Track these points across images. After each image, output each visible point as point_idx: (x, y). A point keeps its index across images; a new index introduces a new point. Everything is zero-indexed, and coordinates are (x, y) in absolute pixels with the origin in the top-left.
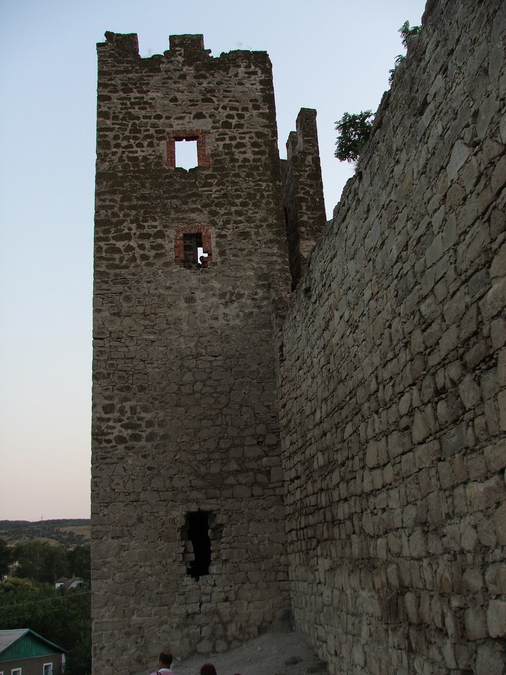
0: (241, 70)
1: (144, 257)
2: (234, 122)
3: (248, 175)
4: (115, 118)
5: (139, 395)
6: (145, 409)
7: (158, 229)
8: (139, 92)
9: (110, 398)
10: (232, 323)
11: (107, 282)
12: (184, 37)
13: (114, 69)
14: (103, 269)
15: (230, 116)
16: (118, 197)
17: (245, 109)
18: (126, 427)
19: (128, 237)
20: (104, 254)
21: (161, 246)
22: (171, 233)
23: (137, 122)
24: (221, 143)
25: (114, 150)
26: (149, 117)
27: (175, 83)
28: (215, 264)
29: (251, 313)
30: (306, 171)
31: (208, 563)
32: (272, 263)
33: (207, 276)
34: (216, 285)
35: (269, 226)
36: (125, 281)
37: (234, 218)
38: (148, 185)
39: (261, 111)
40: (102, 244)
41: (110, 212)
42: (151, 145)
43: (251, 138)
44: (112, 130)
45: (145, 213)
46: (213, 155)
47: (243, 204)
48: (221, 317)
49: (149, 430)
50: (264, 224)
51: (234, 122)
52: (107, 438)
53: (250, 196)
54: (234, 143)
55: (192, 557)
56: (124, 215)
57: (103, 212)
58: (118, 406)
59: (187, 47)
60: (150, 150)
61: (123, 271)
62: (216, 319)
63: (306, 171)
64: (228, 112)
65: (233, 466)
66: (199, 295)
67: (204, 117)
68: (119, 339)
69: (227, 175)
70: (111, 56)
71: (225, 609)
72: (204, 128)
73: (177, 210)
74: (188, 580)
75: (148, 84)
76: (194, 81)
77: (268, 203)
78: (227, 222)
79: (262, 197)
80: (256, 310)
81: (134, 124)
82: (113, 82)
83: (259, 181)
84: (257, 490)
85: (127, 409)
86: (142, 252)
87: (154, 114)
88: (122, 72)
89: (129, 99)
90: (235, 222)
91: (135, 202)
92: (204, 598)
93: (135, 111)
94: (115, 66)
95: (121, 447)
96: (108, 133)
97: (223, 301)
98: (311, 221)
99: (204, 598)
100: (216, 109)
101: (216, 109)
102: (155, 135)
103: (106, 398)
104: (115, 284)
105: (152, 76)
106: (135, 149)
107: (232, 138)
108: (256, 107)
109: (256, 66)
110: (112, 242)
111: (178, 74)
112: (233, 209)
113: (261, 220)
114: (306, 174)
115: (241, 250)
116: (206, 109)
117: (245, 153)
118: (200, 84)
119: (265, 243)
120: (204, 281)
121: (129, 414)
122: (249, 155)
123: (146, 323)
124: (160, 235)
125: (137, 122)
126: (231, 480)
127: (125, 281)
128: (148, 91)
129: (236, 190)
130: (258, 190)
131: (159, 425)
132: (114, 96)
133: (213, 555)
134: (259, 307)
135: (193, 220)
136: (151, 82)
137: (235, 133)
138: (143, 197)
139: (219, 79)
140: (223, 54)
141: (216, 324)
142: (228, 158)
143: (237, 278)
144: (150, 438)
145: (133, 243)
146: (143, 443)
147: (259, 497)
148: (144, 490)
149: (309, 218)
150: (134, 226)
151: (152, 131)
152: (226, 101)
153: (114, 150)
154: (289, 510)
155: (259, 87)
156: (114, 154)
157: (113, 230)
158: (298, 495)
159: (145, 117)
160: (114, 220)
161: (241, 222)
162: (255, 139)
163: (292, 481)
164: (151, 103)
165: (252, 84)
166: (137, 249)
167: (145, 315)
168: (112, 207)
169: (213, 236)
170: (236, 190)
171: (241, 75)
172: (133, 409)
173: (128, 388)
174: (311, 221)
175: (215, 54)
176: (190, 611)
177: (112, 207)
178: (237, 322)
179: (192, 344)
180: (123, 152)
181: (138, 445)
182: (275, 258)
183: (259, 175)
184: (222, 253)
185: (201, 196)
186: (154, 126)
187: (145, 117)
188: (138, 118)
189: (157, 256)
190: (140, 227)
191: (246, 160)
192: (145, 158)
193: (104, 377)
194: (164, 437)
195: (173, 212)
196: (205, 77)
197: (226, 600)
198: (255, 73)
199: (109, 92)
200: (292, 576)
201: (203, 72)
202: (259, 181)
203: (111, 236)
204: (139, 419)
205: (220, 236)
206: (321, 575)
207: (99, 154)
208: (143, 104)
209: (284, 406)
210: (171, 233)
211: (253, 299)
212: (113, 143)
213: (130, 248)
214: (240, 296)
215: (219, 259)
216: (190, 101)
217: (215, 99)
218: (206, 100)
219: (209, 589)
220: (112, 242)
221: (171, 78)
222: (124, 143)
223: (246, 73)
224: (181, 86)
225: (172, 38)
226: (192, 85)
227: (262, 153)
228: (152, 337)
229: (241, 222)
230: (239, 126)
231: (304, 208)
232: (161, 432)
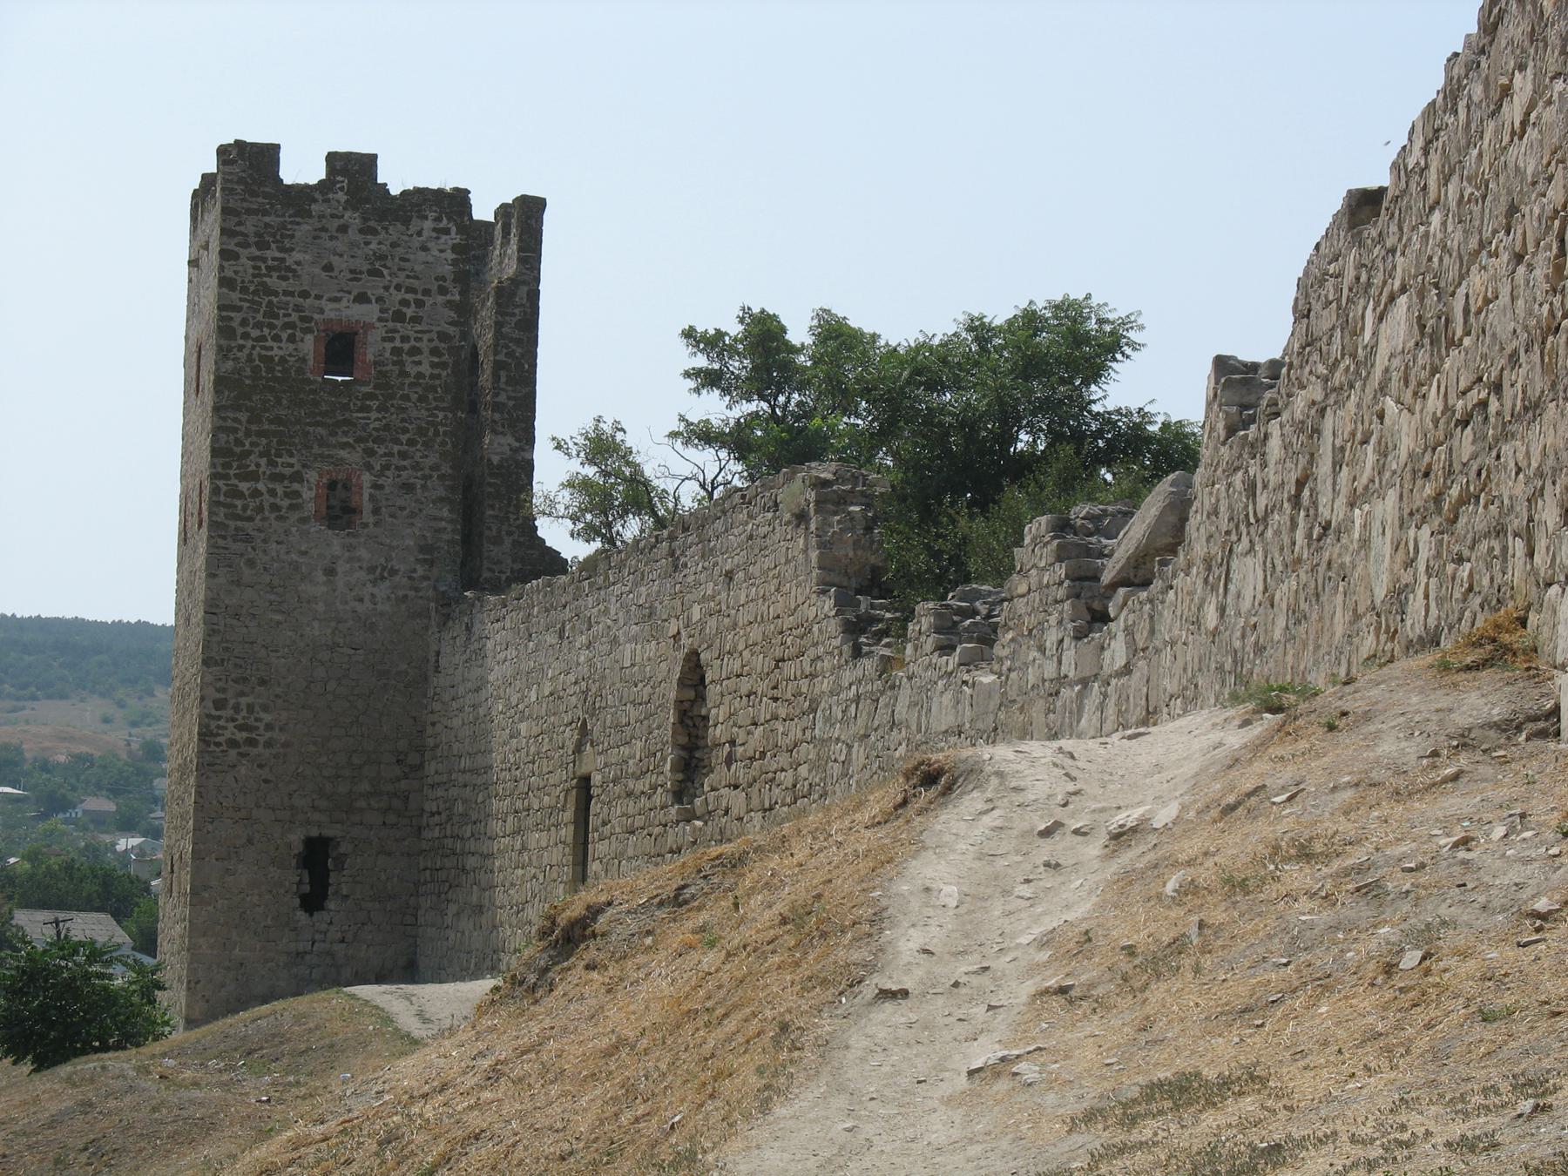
0: (428, 225)
1: (275, 508)
2: (409, 312)
3: (420, 399)
4: (244, 290)
5: (258, 689)
6: (265, 708)
7: (297, 467)
8: (281, 250)
9: (224, 690)
10: (379, 607)
11: (224, 538)
12: (349, 156)
13: (245, 205)
14: (220, 518)
15: (405, 303)
16: (243, 416)
17: (427, 292)
18: (241, 728)
19: (253, 476)
20: (222, 498)
21: (297, 494)
22: (312, 476)
23: (275, 300)
24: (389, 346)
25: (241, 342)
26: (292, 294)
27: (331, 238)
28: (366, 525)
29: (406, 596)
30: (514, 315)
31: (325, 896)
32: (438, 531)
33: (352, 540)
34: (363, 553)
35: (442, 477)
36: (248, 539)
37: (396, 461)
38: (285, 402)
39: (449, 297)
40: (221, 483)
41: (232, 437)
42: (292, 339)
43: (430, 340)
44: (238, 309)
45: (280, 443)
46: (375, 363)
47: (411, 442)
48: (367, 599)
49: (268, 735)
50: (435, 475)
51: (409, 312)
52: (218, 739)
53: (421, 431)
54: (406, 346)
55: (306, 889)
56: (252, 444)
57: (223, 437)
58: (232, 702)
59: (353, 171)
60: (292, 347)
61: (246, 524)
62: (361, 600)
63: (514, 315)
64: (402, 295)
65: (365, 787)
66: (342, 567)
67: (368, 301)
68: (237, 616)
69: (392, 397)
70: (240, 181)
71: (339, 948)
72: (367, 320)
73: (322, 443)
74: (302, 916)
75: (292, 237)
76: (359, 238)
77: (443, 443)
78: (386, 467)
79: (437, 433)
80: (412, 593)
81: (270, 302)
82: (242, 228)
83: (436, 408)
84: (391, 819)
85: (243, 707)
86: (272, 500)
87: (298, 289)
88: (255, 212)
89: (264, 260)
90: (397, 468)
91: (266, 427)
92: (318, 937)
93: (273, 281)
94: (243, 200)
95: (233, 753)
96: (233, 315)
97: (371, 577)
98: (511, 403)
99: (318, 937)
100: (386, 288)
101: (386, 288)
102: (299, 324)
103: (218, 690)
104: (235, 541)
105: (298, 224)
106: (270, 343)
107: (405, 339)
108: (443, 291)
109: (449, 219)
110: (234, 481)
111: (336, 223)
112: (396, 448)
113: (431, 468)
114: (514, 320)
115: (402, 509)
116: (374, 287)
117: (420, 363)
118: (367, 244)
119: (434, 502)
120: (350, 548)
121: (244, 713)
122: (425, 369)
123: (273, 597)
124: (297, 477)
125: (275, 300)
126: (361, 803)
127: (248, 539)
128: (292, 249)
129: (403, 420)
130: (434, 424)
131: (281, 729)
132: (243, 252)
133: (331, 890)
134: (417, 590)
135: (342, 459)
136: (298, 234)
137: (407, 329)
138: (278, 420)
139: (394, 238)
140: (404, 193)
141: (360, 608)
142: (396, 369)
143: (392, 548)
144: (268, 744)
145: (261, 486)
146: (260, 748)
147: (393, 826)
148: (258, 806)
149: (509, 398)
150: (263, 461)
151: (294, 317)
152: (402, 275)
153: (241, 342)
154: (424, 845)
155: (450, 255)
156: (241, 348)
157: (235, 465)
158: (436, 834)
159: (286, 293)
160: (238, 450)
161: (405, 468)
162: (436, 343)
163: (433, 814)
164: (295, 271)
165: (442, 251)
166: (266, 496)
167: (271, 586)
168: (235, 430)
169: (366, 485)
170: (403, 420)
171: (425, 234)
172: (250, 708)
173: (245, 680)
174: (511, 403)
175: (395, 190)
176: (301, 949)
177: (235, 430)
178: (387, 608)
179: (329, 631)
180: (253, 348)
181: (254, 751)
182: (443, 524)
183: (435, 399)
184: (376, 511)
185: (355, 425)
186: (298, 308)
187: (286, 293)
188: (276, 294)
189: (292, 507)
190: (272, 463)
191: (420, 375)
192: (283, 360)
193: (216, 664)
194: (286, 745)
195: (316, 446)
196: (374, 232)
197: (342, 941)
198: (447, 231)
199: (237, 245)
200: (421, 920)
201: (372, 223)
202: (436, 408)
203: (232, 472)
204: (256, 720)
205: (376, 486)
206: (448, 920)
207: (220, 348)
208: (286, 271)
209: (433, 724)
210: (312, 476)
211: (410, 578)
212: (240, 331)
213: (256, 493)
214: (393, 572)
215: (371, 520)
216: (352, 271)
217: (385, 272)
218: (374, 273)
219: (324, 926)
220: (234, 481)
221: (326, 230)
222: (255, 333)
223: (434, 230)
224: (341, 247)
225: (332, 158)
226: (353, 245)
227: (443, 365)
228: (278, 617)
229: (405, 468)
230: (416, 319)
231: (503, 379)
232: (283, 738)
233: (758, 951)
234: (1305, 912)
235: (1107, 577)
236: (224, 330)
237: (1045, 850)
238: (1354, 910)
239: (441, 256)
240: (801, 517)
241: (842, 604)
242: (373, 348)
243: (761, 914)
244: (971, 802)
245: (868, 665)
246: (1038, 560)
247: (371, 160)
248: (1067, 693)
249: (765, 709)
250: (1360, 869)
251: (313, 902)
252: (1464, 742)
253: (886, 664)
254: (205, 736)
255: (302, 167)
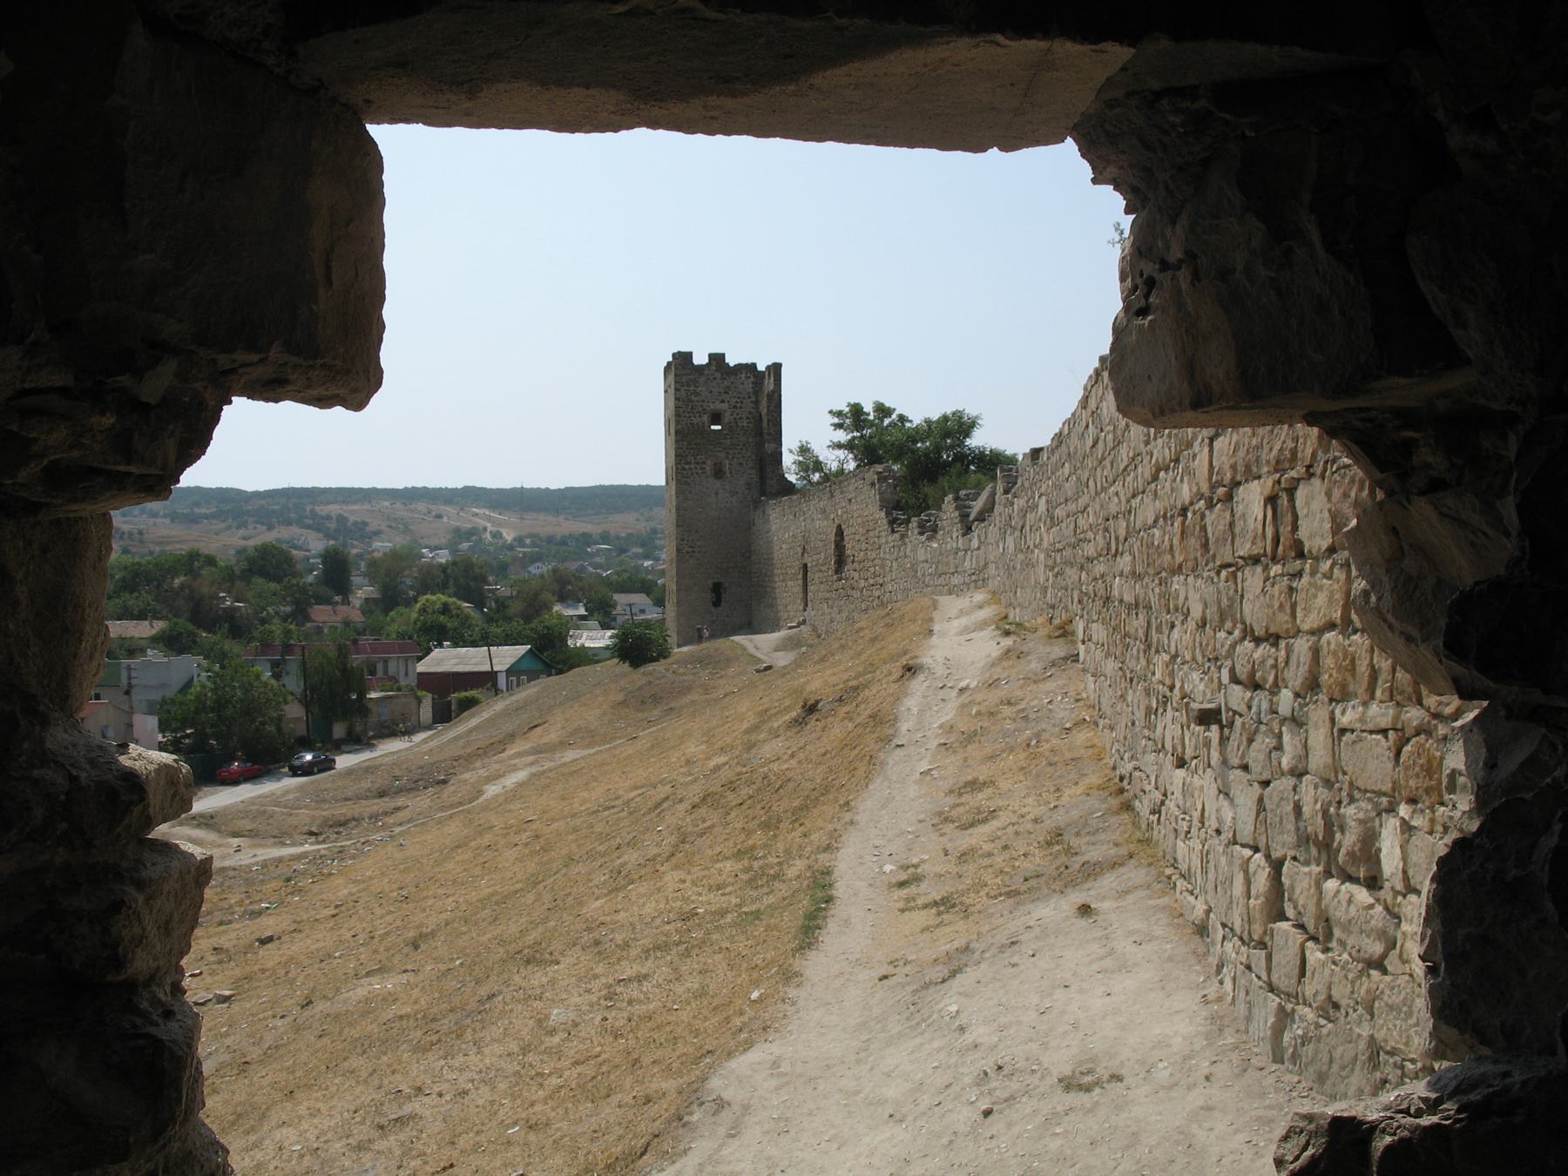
59: (717, 359)
208: (696, 394)
225: (710, 356)
233: (865, 725)
234: (1009, 725)
235: (972, 517)
236: (678, 415)
237: (941, 694)
238: (1020, 724)
239: (748, 386)
240: (873, 484)
241: (888, 514)
242: (727, 418)
243: (865, 712)
244: (921, 677)
245: (897, 536)
246: (948, 512)
247: (722, 356)
248: (961, 554)
249: (864, 546)
250: (1023, 710)
251: (717, 604)
252: (1053, 664)
253: (903, 537)
254: (678, 550)
255: (700, 359)
